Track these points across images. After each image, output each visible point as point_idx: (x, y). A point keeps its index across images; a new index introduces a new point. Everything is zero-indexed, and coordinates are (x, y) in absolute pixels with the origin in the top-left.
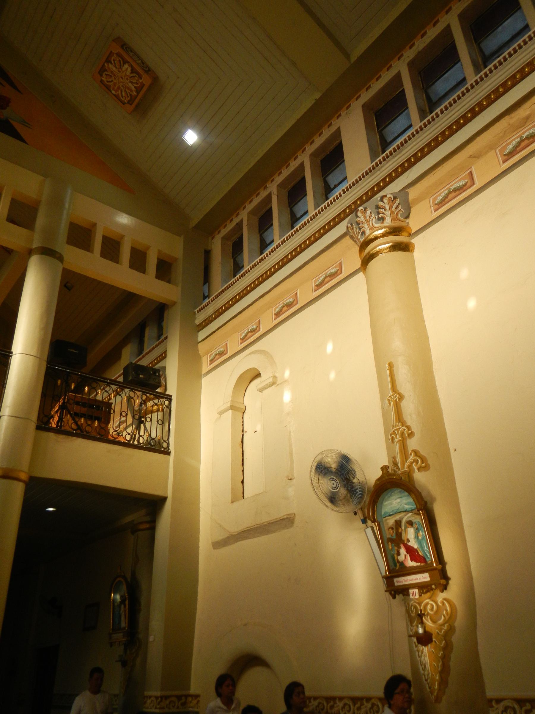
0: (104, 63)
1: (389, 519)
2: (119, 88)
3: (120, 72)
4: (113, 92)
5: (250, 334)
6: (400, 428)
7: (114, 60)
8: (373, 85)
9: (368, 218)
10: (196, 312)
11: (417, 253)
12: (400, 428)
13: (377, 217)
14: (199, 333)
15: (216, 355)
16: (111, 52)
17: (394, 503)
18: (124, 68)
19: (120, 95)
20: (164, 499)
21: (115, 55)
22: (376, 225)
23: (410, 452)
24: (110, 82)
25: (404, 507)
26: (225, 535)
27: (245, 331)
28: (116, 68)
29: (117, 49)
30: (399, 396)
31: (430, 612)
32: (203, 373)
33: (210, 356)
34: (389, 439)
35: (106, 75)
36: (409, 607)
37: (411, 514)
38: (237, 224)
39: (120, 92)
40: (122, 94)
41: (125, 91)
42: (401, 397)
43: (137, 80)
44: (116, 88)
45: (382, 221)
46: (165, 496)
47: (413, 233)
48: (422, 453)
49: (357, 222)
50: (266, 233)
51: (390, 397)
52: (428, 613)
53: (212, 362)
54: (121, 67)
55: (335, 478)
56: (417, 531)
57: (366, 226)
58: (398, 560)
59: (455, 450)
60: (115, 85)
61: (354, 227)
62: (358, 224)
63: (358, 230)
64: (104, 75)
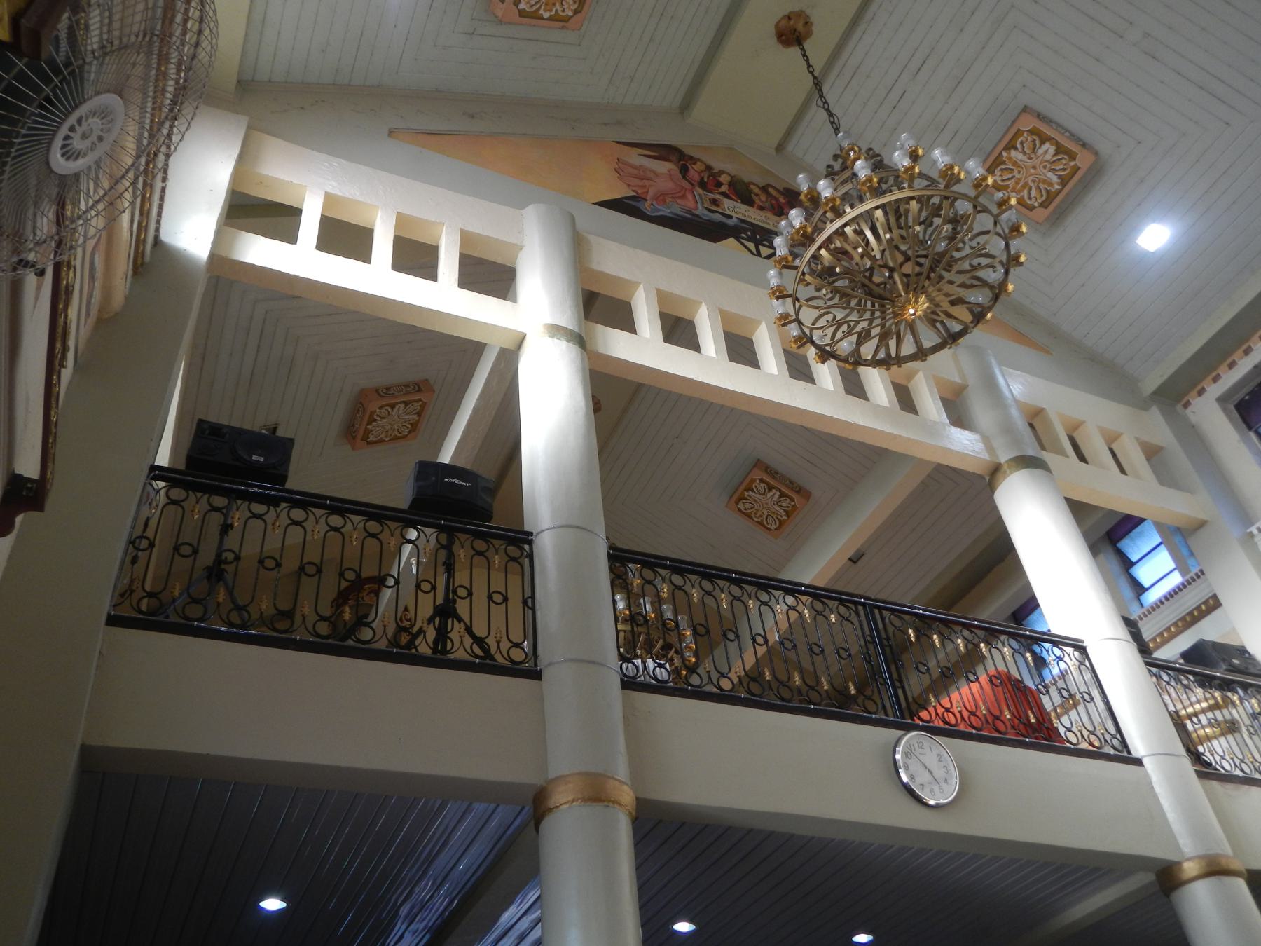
0: (1001, 153)
2: (1026, 184)
7: (1022, 143)
10: (1255, 532)
16: (1019, 130)
18: (1040, 152)
24: (1009, 179)
28: (1024, 153)
35: (1002, 170)
38: (1256, 367)
39: (1025, 192)
40: (1030, 194)
41: (1038, 188)
43: (1065, 165)
44: (1019, 186)
54: (1034, 150)
60: (1017, 183)
64: (998, 172)
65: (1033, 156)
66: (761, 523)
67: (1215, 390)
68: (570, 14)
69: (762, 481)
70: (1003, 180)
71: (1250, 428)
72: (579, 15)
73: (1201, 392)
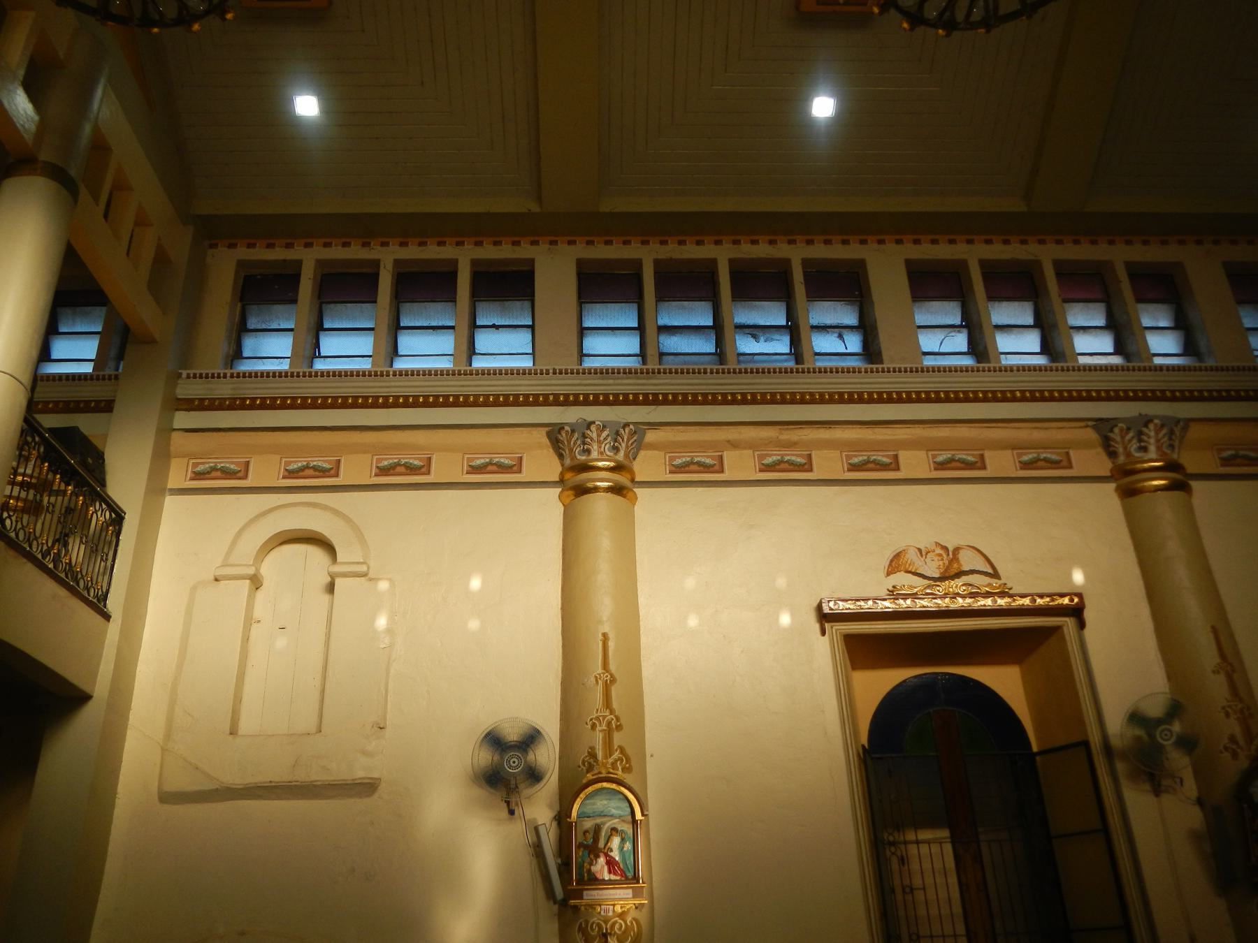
1: (587, 821)
5: (311, 472)
6: (607, 716)
8: (598, 246)
9: (602, 438)
10: (184, 375)
11: (638, 509)
12: (607, 716)
13: (612, 444)
14: (177, 413)
15: (214, 469)
17: (598, 804)
20: (84, 698)
22: (608, 453)
23: (615, 748)
25: (610, 811)
26: (208, 786)
27: (301, 461)
30: (611, 677)
31: (617, 931)
32: (170, 486)
33: (195, 465)
34: (587, 723)
36: (587, 926)
37: (617, 820)
38: (285, 260)
42: (613, 680)
45: (615, 451)
46: (92, 694)
47: (637, 482)
48: (629, 751)
49: (584, 434)
50: (332, 306)
51: (600, 674)
52: (615, 932)
53: (198, 477)
55: (512, 753)
56: (623, 840)
57: (595, 446)
58: (589, 871)
59: (652, 756)
61: (576, 435)
62: (584, 436)
63: (579, 442)
67: (243, 253)
71: (241, 300)
73: (232, 246)
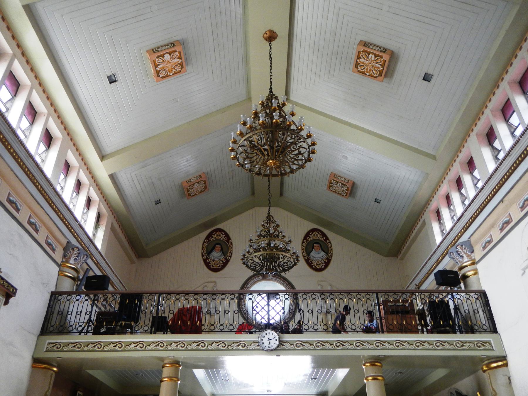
2: (370, 70)
3: (367, 61)
4: (368, 74)
7: (362, 56)
15: (503, 224)
16: (359, 52)
18: (370, 58)
19: (372, 73)
21: (362, 53)
28: (365, 59)
29: (362, 48)
35: (360, 66)
39: (371, 72)
40: (373, 73)
43: (380, 60)
60: (367, 70)
64: (359, 67)
65: (368, 59)
66: (340, 194)
68: (180, 70)
69: (334, 180)
70: (362, 70)
72: (183, 69)
